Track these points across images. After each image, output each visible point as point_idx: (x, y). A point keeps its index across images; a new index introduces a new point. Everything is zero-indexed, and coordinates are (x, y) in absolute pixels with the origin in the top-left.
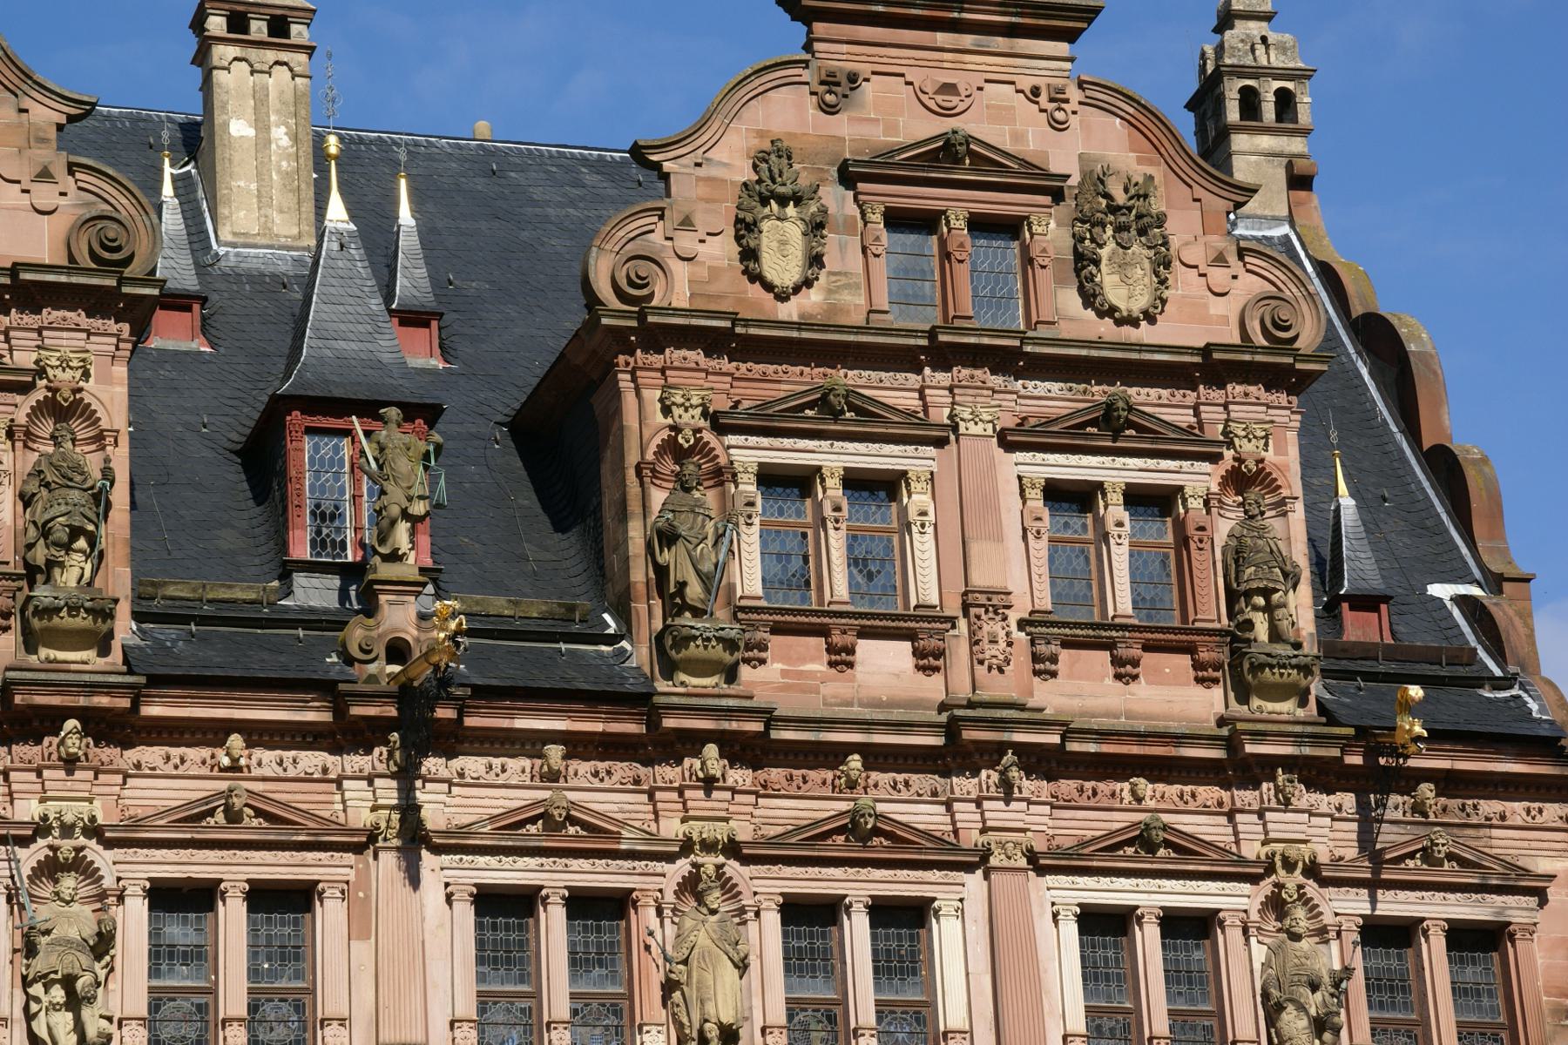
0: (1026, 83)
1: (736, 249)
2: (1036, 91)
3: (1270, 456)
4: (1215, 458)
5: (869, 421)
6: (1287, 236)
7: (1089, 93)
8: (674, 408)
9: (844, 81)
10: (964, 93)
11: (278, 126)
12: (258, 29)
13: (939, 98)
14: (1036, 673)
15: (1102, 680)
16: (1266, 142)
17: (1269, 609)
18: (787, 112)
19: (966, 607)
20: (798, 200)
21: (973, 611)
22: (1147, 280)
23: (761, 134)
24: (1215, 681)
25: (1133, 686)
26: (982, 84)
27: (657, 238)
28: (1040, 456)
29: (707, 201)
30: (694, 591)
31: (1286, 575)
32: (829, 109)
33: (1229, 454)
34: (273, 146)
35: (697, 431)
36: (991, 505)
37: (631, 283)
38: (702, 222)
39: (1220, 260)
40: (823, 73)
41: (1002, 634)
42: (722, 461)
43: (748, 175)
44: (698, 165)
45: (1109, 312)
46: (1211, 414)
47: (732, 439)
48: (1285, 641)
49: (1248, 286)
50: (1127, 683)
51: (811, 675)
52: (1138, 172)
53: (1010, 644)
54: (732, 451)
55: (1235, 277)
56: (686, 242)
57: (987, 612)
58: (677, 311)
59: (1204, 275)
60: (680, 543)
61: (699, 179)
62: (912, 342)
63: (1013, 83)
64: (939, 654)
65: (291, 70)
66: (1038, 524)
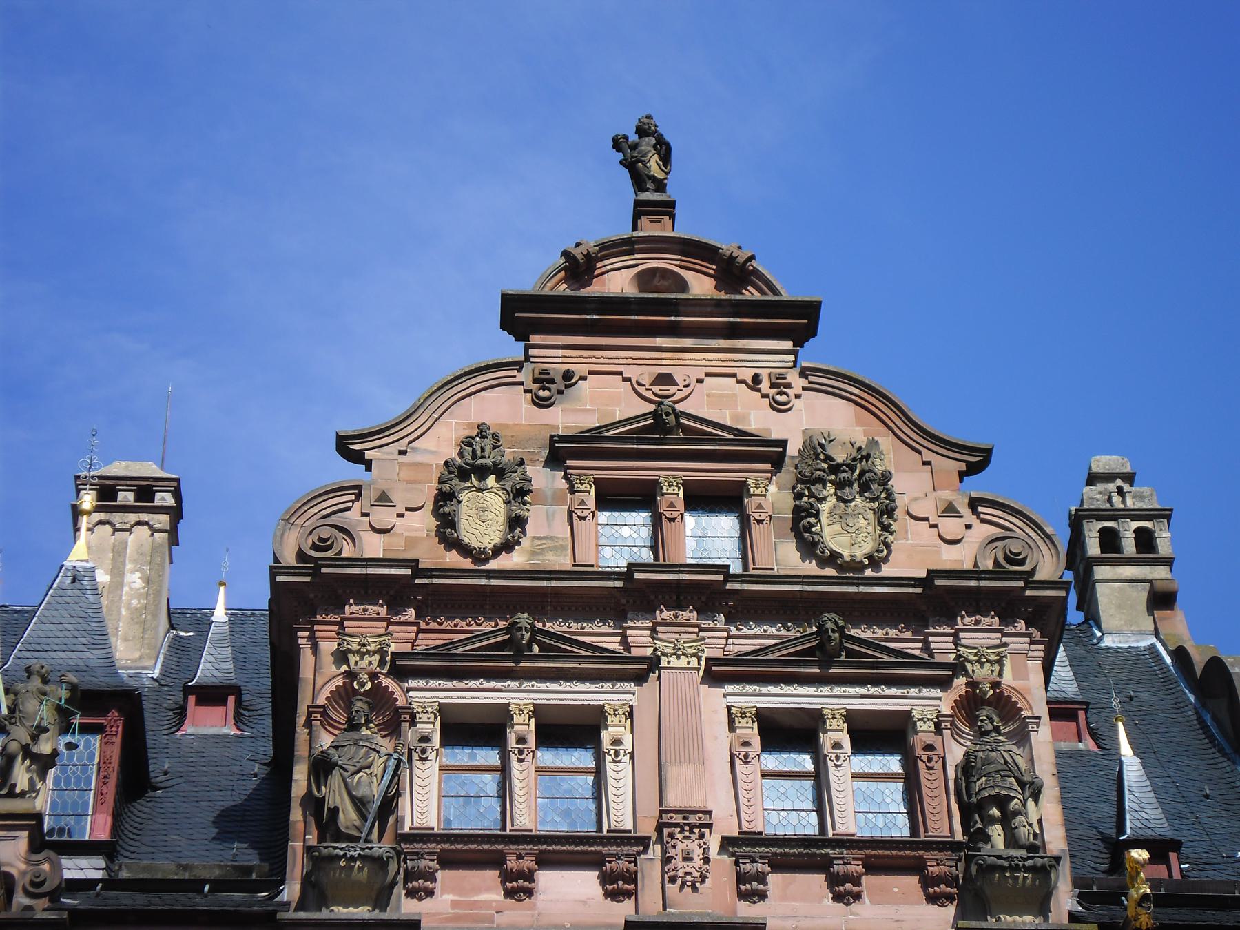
0: (747, 375)
1: (433, 523)
2: (756, 379)
3: (1008, 678)
4: (944, 684)
5: (561, 662)
6: (1153, 646)
7: (811, 378)
8: (350, 656)
9: (559, 379)
10: (681, 384)
11: (133, 572)
12: (126, 497)
13: (656, 389)
14: (743, 896)
15: (821, 901)
16: (1129, 571)
17: (1006, 820)
18: (506, 409)
19: (660, 828)
20: (500, 472)
21: (666, 831)
22: (870, 529)
23: (470, 425)
24: (950, 898)
25: (855, 907)
26: (702, 376)
27: (354, 514)
28: (749, 688)
29: (409, 482)
30: (348, 817)
31: (1022, 784)
32: (541, 403)
33: (960, 681)
34: (126, 589)
35: (373, 676)
36: (693, 730)
37: (315, 547)
38: (400, 499)
39: (950, 510)
40: (537, 372)
41: (697, 853)
42: (400, 703)
43: (453, 454)
44: (402, 453)
45: (832, 559)
46: (937, 643)
47: (413, 683)
48: (1021, 847)
49: (983, 531)
50: (848, 904)
51: (487, 904)
52: (861, 441)
53: (706, 860)
54: (411, 693)
55: (968, 527)
56: (382, 517)
57: (682, 831)
58: (351, 562)
59: (935, 526)
60: (336, 771)
61: (401, 465)
62: (610, 584)
63: (734, 375)
64: (632, 878)
65: (151, 527)
66: (747, 749)
